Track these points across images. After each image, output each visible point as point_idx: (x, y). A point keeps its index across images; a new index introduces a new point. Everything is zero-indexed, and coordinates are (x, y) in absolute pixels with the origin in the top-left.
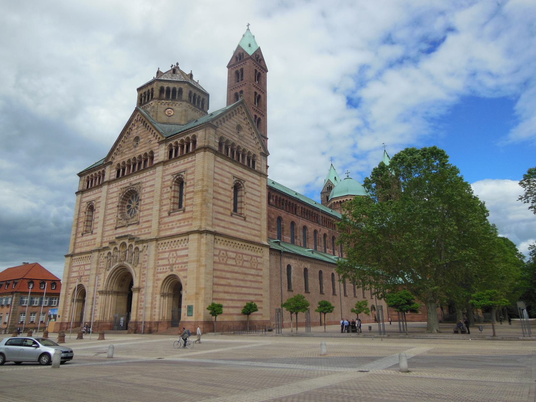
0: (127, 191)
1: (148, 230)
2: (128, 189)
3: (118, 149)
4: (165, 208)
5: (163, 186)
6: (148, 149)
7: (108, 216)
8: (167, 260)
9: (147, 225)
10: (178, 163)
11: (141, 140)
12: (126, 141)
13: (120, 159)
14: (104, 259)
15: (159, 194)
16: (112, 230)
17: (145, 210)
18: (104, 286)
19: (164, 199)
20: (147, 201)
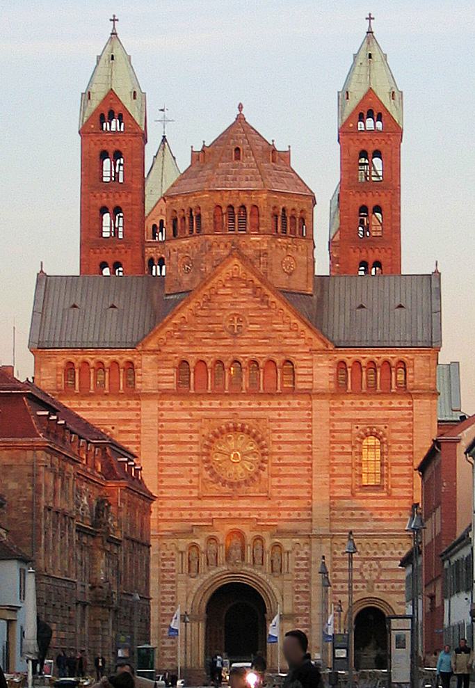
0: (223, 427)
1: (299, 515)
2: (227, 424)
3: (175, 324)
4: (340, 481)
5: (332, 439)
6: (275, 353)
7: (166, 468)
8: (359, 573)
9: (296, 506)
10: (366, 403)
11: (251, 326)
12: (200, 313)
13: (185, 349)
14: (173, 554)
15: (327, 453)
16: (188, 498)
17: (285, 476)
18: (190, 606)
19: (336, 464)
20: (287, 459)
